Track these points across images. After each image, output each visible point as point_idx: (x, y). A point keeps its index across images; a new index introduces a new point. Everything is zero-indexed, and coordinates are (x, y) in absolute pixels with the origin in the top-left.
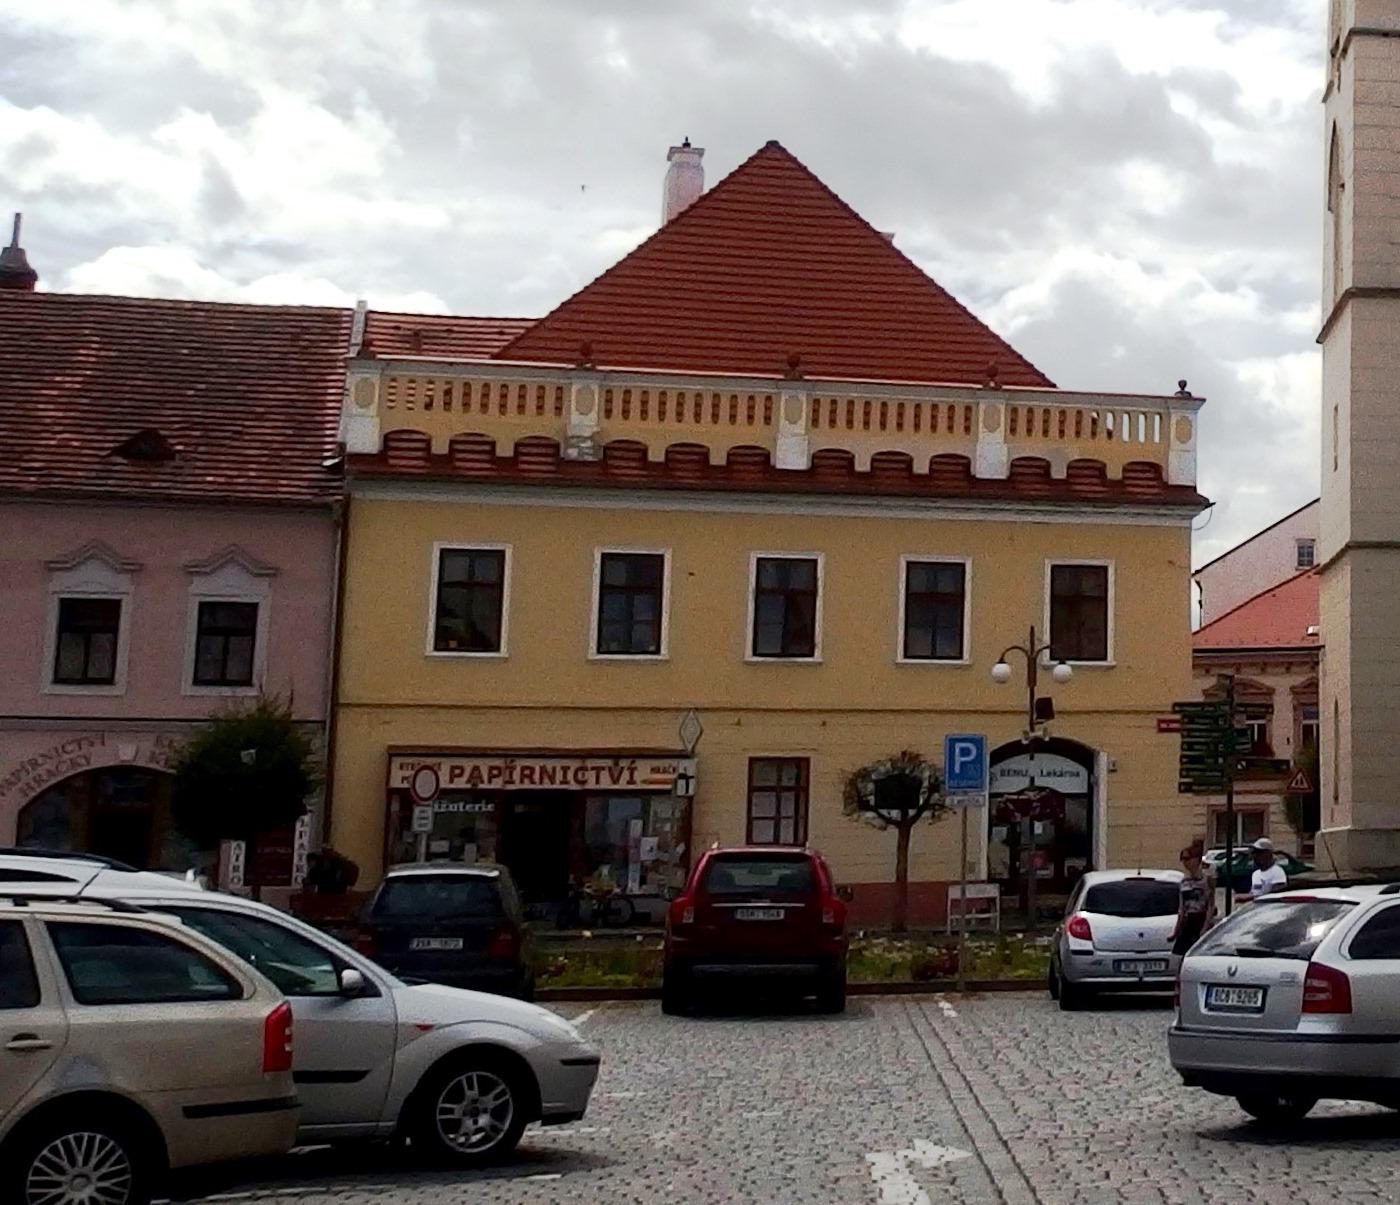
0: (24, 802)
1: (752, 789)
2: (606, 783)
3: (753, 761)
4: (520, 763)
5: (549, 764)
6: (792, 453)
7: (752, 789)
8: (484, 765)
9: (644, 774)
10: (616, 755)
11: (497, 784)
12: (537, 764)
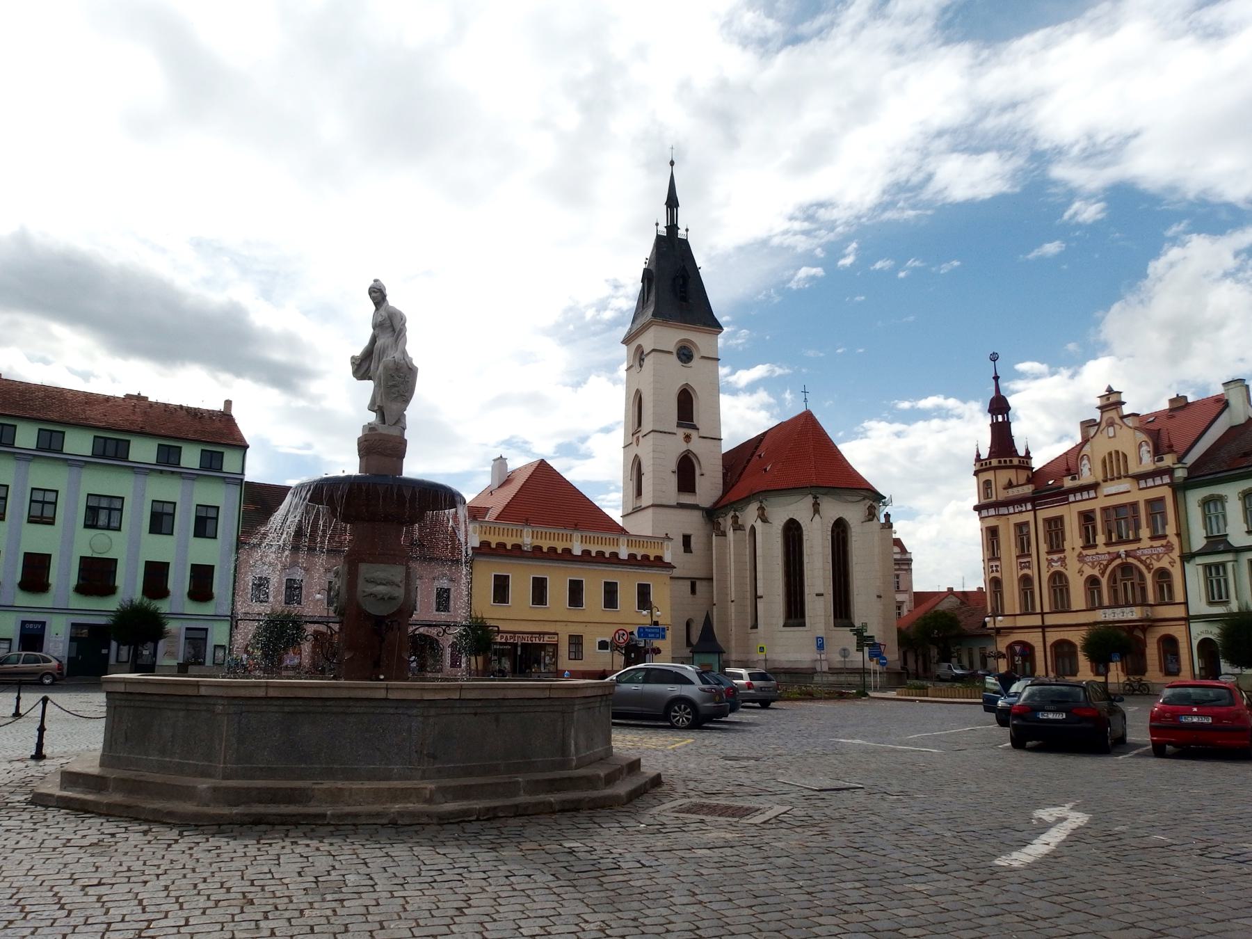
1: (570, 644)
3: (570, 636)
5: (524, 636)
6: (577, 551)
8: (509, 635)
9: (546, 639)
10: (540, 633)
11: (512, 641)
12: (521, 635)
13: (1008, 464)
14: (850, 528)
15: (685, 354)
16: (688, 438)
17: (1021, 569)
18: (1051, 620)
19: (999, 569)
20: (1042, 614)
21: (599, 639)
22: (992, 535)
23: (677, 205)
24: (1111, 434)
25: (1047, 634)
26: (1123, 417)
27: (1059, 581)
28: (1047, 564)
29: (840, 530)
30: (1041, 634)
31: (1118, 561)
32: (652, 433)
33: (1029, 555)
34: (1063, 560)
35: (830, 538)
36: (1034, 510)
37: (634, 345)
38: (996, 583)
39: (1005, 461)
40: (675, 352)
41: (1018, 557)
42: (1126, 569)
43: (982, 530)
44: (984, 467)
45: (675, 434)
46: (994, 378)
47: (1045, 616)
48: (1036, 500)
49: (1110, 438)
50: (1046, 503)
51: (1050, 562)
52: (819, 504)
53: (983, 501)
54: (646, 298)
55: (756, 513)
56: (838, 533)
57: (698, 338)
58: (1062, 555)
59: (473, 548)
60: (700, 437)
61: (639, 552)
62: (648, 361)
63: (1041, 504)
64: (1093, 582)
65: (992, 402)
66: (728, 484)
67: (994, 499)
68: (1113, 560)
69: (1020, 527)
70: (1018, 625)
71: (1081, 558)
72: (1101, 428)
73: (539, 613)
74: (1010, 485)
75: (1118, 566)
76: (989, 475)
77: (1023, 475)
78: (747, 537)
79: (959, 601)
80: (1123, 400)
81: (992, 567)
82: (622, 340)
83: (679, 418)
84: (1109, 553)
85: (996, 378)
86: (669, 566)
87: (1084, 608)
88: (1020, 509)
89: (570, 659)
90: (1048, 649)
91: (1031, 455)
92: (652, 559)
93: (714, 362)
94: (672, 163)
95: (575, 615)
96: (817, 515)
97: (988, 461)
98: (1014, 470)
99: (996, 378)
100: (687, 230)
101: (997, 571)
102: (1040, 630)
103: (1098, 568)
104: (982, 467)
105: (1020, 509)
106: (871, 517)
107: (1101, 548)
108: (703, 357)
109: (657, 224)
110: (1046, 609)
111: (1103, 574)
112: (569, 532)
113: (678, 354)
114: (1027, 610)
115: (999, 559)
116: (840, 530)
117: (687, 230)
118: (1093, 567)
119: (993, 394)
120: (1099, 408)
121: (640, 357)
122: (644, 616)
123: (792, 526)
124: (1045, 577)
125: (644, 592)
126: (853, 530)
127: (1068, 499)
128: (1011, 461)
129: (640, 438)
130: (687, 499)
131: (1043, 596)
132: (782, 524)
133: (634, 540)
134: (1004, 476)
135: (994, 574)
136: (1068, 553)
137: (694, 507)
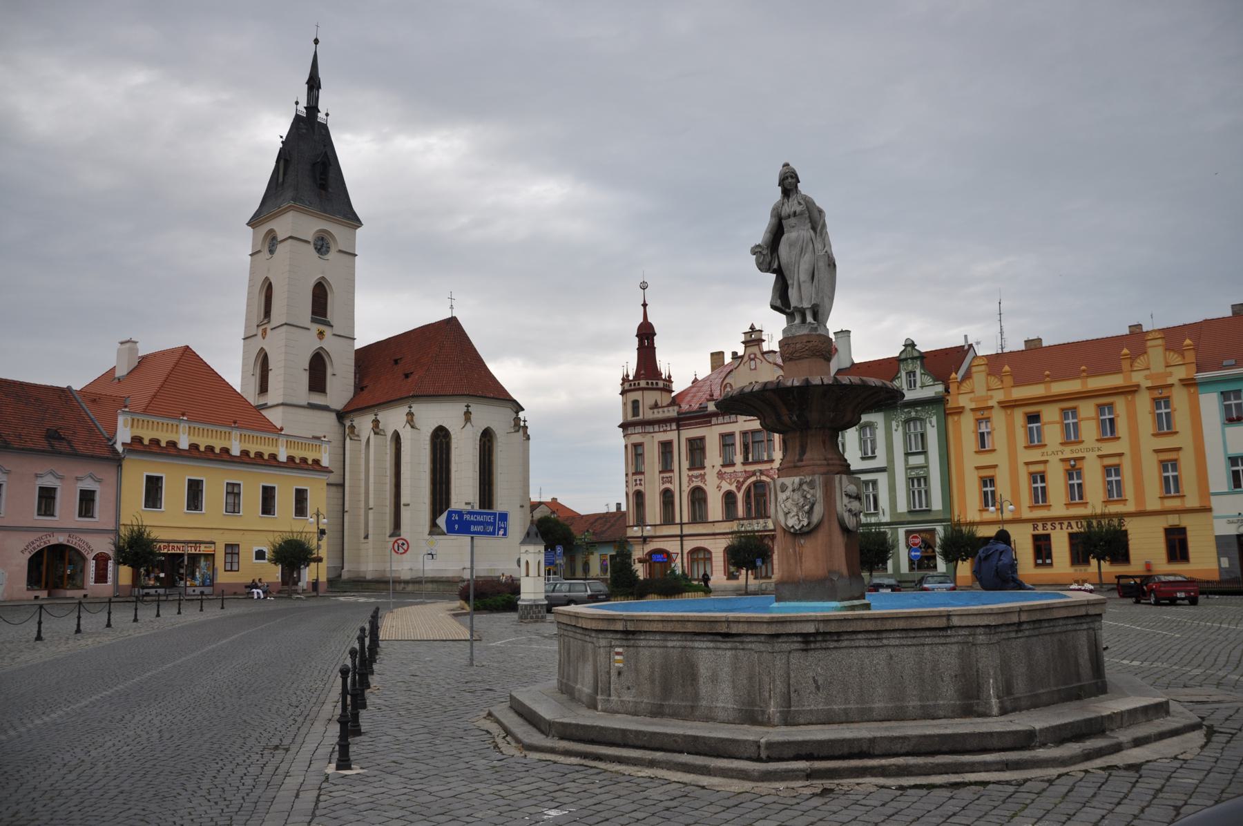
0: (30, 556)
2: (193, 552)
3: (226, 545)
4: (171, 544)
5: (179, 545)
7: (226, 553)
9: (203, 549)
10: (196, 542)
11: (166, 551)
12: (175, 545)
13: (655, 386)
14: (496, 438)
15: (322, 245)
16: (321, 334)
17: (663, 484)
18: (687, 530)
19: (643, 482)
20: (681, 524)
21: (256, 549)
22: (636, 453)
23: (319, 87)
24: (753, 367)
25: (685, 543)
26: (763, 353)
27: (698, 497)
28: (688, 479)
29: (487, 438)
30: (679, 543)
31: (753, 479)
32: (285, 326)
33: (672, 471)
34: (703, 477)
35: (478, 447)
36: (678, 429)
37: (265, 228)
38: (639, 498)
39: (652, 383)
40: (312, 243)
41: (660, 472)
42: (759, 485)
43: (626, 447)
44: (633, 387)
45: (309, 329)
46: (643, 305)
47: (684, 526)
48: (681, 421)
49: (751, 369)
50: (689, 425)
51: (690, 478)
52: (470, 413)
53: (630, 418)
54: (281, 180)
55: (405, 418)
56: (484, 442)
57: (337, 230)
58: (702, 472)
59: (123, 444)
60: (334, 335)
61: (298, 454)
62: (281, 249)
63: (685, 425)
64: (729, 498)
65: (641, 328)
66: (359, 388)
67: (641, 417)
68: (748, 478)
69: (666, 447)
70: (658, 534)
71: (720, 475)
72: (744, 361)
73: (194, 519)
74: (656, 406)
75: (755, 483)
76: (636, 395)
77: (665, 399)
78: (388, 443)
79: (550, 511)
80: (764, 338)
81: (636, 480)
82: (247, 222)
83: (313, 313)
84: (745, 471)
85: (645, 305)
86: (326, 470)
87: (721, 519)
88: (665, 428)
89: (225, 571)
90: (685, 556)
91: (672, 379)
92: (310, 462)
93: (351, 257)
94: (316, 42)
95: (233, 522)
96: (469, 424)
97: (637, 382)
98: (659, 392)
99: (645, 305)
100: (327, 115)
101: (641, 484)
102: (679, 539)
103: (735, 484)
104: (628, 386)
105: (665, 428)
106: (517, 428)
107: (739, 467)
108: (340, 251)
109: (297, 103)
110: (685, 520)
111: (739, 489)
112: (228, 430)
113: (315, 244)
114: (668, 519)
115: (642, 473)
116: (487, 438)
117: (327, 115)
118: (731, 484)
119: (641, 320)
120: (743, 342)
121: (272, 242)
122: (311, 523)
123: (439, 433)
124: (686, 490)
125: (301, 496)
126: (499, 440)
127: (710, 422)
128: (657, 383)
129: (268, 330)
130: (317, 399)
131: (683, 509)
132: (431, 431)
133: (292, 440)
134: (650, 398)
135: (638, 487)
136: (708, 470)
137: (325, 408)
